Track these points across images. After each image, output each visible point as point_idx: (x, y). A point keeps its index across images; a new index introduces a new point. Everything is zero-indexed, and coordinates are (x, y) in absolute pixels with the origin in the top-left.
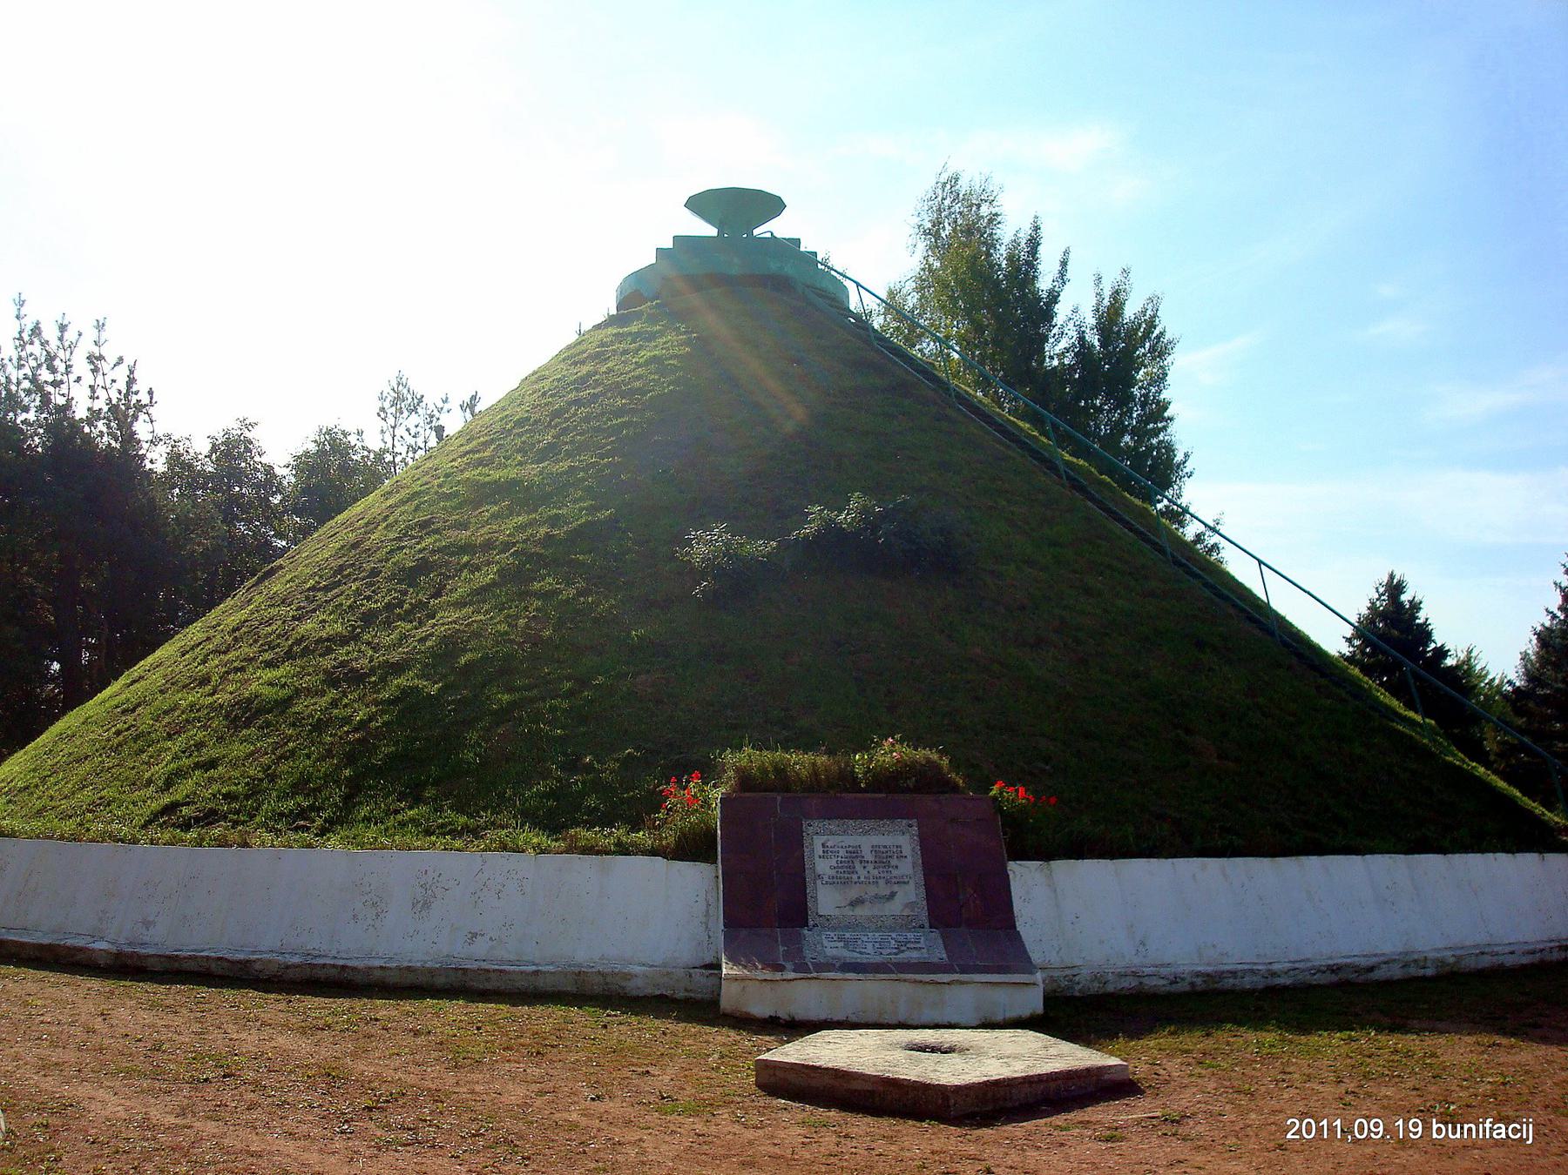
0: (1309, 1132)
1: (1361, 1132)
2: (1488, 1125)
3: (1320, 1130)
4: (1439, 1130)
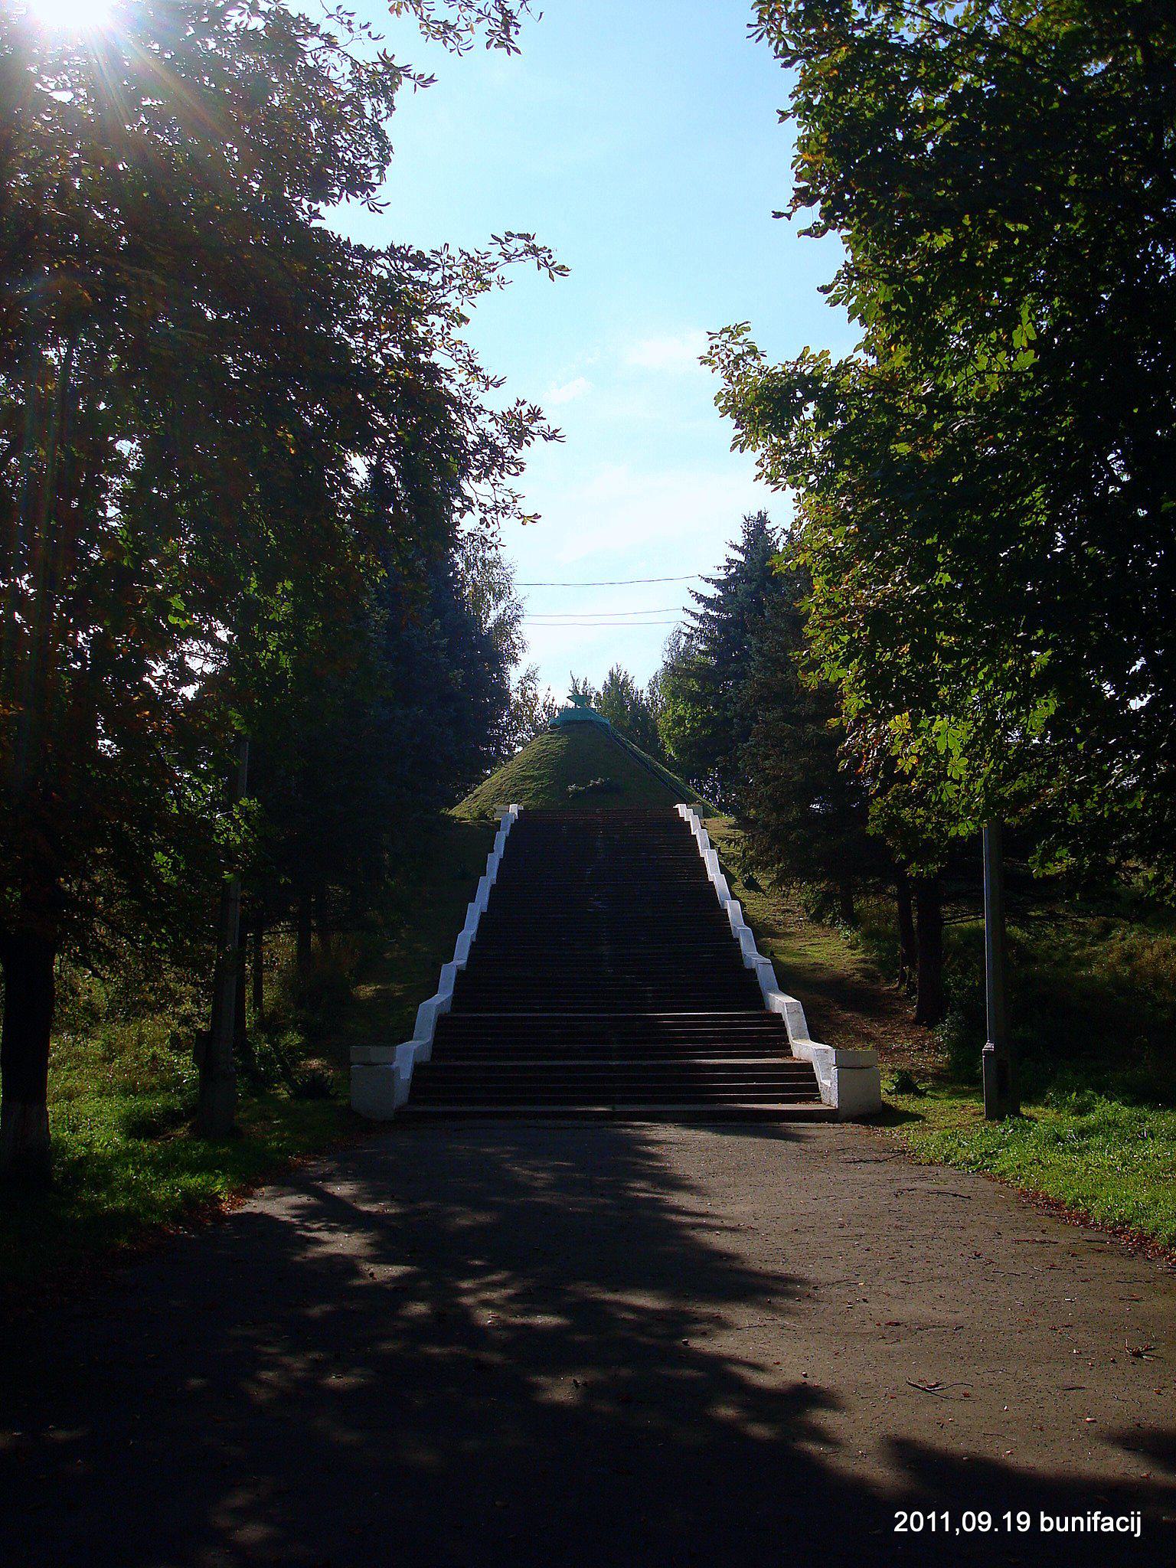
0: (917, 1525)
1: (969, 1525)
2: (1096, 1518)
3: (928, 1522)
4: (1047, 1524)
